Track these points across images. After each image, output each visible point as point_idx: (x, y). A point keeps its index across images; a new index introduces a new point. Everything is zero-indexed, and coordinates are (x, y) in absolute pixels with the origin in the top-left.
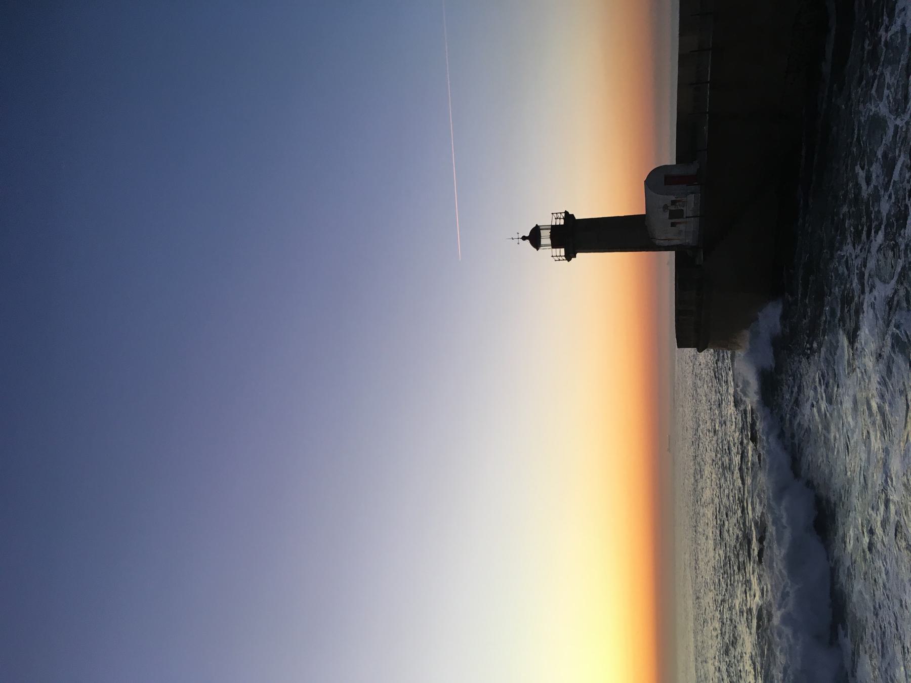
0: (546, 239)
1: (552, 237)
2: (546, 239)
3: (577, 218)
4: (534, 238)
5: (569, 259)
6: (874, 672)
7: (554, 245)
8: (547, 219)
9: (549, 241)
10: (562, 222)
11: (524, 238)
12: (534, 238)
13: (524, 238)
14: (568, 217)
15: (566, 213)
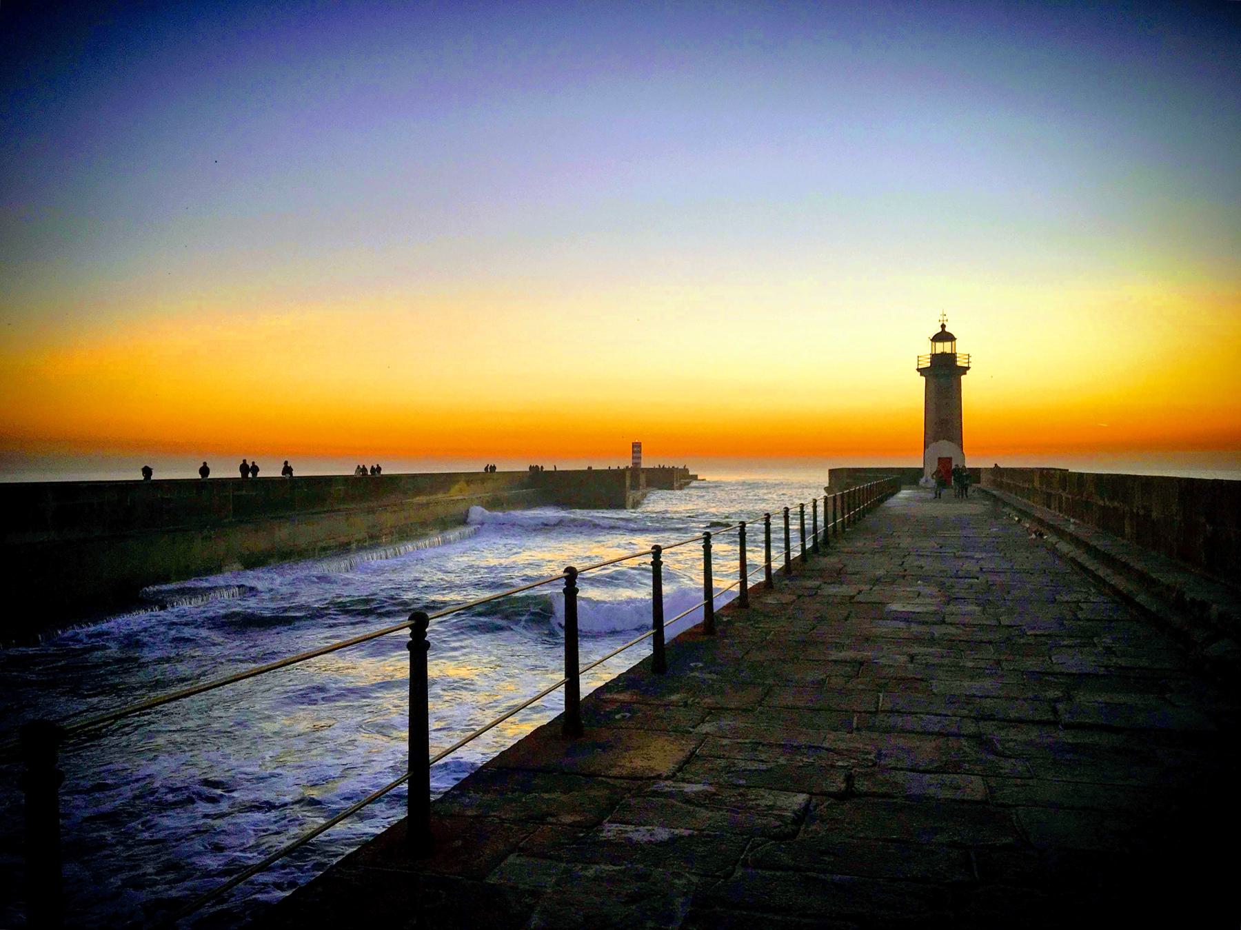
0: (942, 347)
1: (943, 354)
2: (942, 347)
3: (963, 377)
4: (943, 336)
5: (922, 371)
6: (803, 540)
7: (935, 358)
8: (961, 349)
9: (939, 351)
10: (959, 364)
11: (943, 326)
12: (943, 336)
13: (943, 326)
14: (964, 370)
15: (968, 368)
